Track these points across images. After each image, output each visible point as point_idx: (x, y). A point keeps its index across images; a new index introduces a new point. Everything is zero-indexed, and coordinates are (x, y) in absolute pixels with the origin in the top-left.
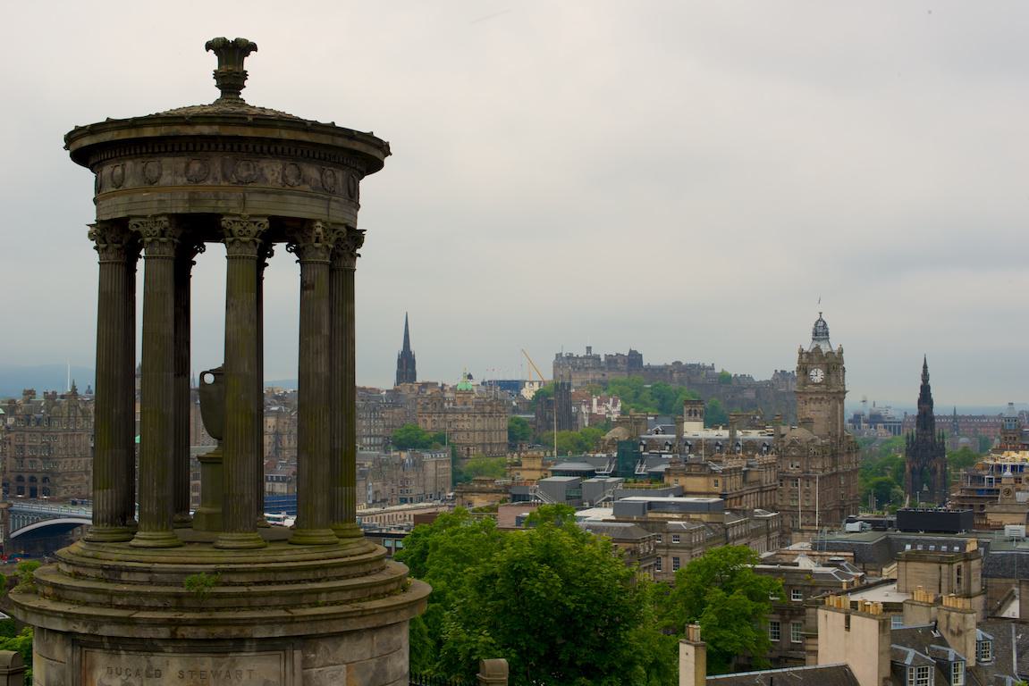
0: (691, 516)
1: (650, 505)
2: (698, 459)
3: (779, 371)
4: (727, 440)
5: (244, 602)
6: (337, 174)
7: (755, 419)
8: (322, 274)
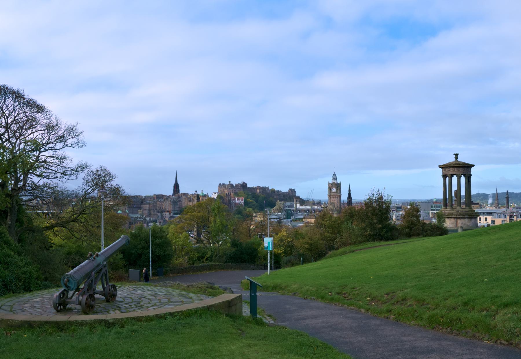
8: (467, 180)
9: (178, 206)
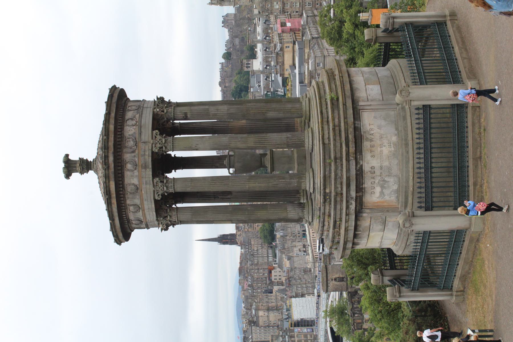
0: (306, 58)
1: (301, 82)
2: (276, 57)
3: (223, 25)
4: (263, 44)
5: (337, 128)
6: (130, 105)
7: (250, 30)
9: (260, 251)
